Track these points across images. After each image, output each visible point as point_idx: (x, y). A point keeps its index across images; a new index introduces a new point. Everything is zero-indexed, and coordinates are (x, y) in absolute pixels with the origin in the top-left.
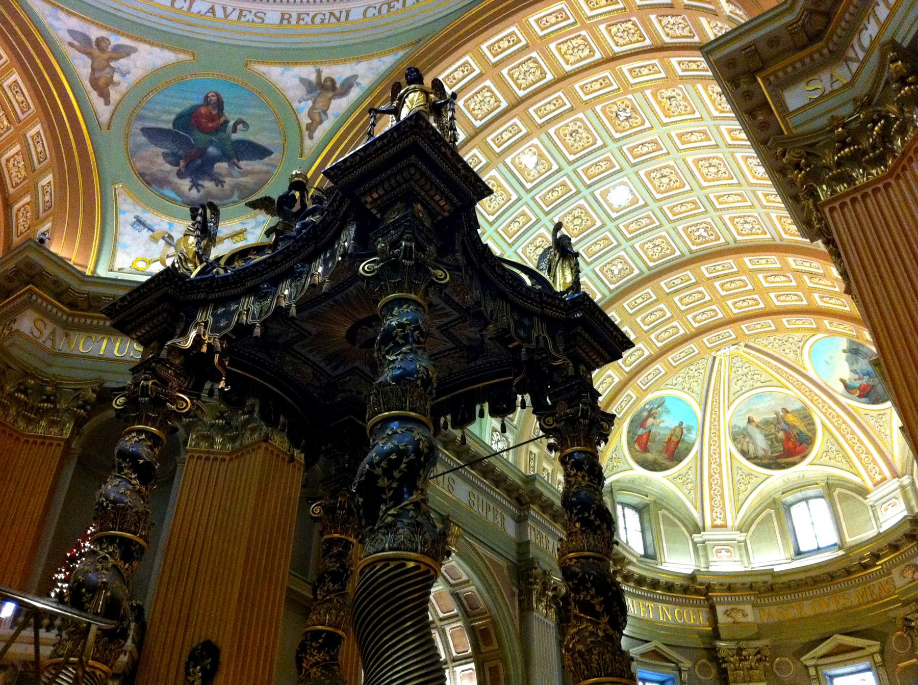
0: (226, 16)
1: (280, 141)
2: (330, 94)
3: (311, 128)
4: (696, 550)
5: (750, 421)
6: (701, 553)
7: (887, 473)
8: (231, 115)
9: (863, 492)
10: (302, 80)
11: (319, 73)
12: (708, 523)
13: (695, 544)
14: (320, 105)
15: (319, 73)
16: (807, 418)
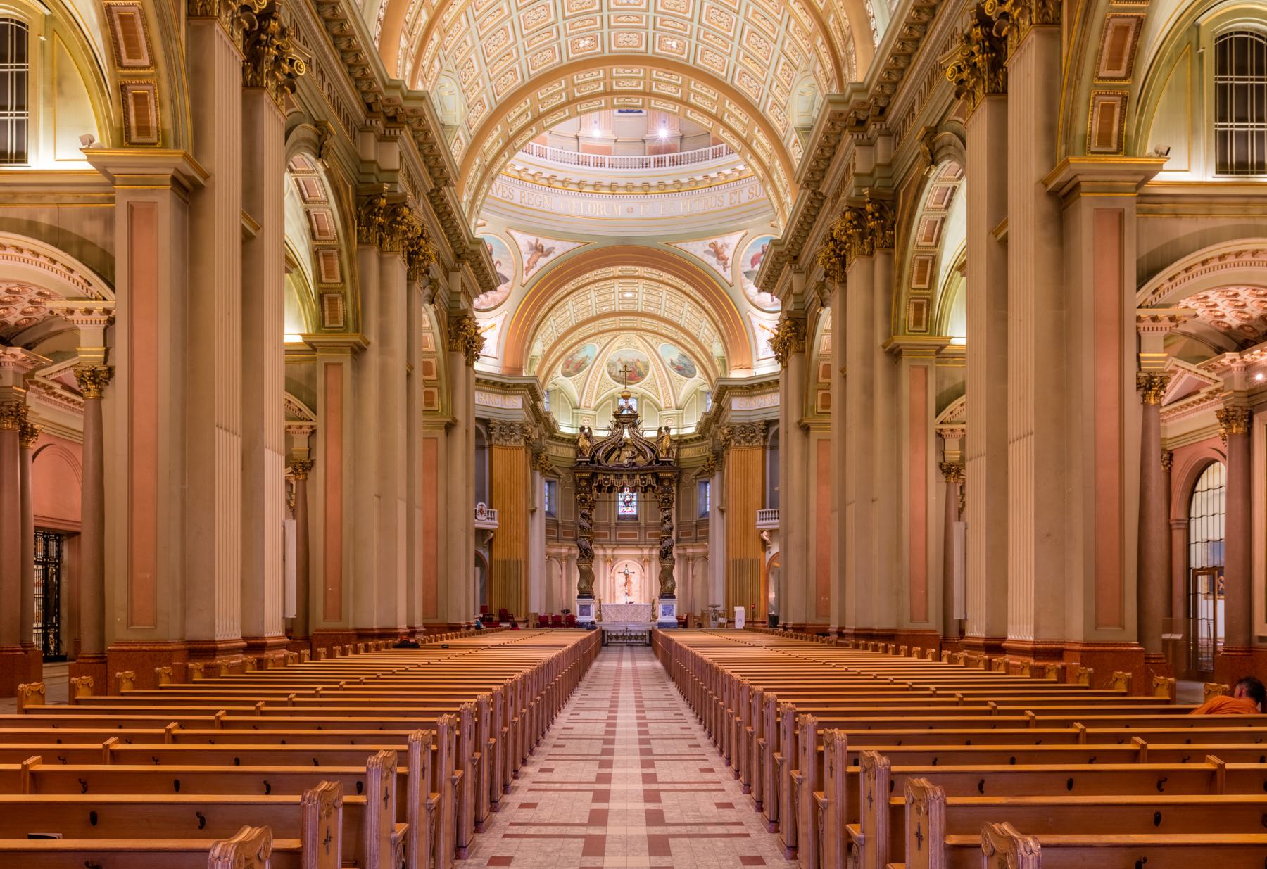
0: (497, 192)
1: (513, 274)
2: (540, 254)
3: (528, 269)
4: (573, 417)
5: (619, 360)
6: (575, 419)
7: (673, 405)
8: (495, 258)
9: (660, 410)
10: (529, 243)
11: (537, 240)
12: (582, 404)
13: (573, 413)
14: (534, 258)
15: (537, 240)
16: (647, 367)
